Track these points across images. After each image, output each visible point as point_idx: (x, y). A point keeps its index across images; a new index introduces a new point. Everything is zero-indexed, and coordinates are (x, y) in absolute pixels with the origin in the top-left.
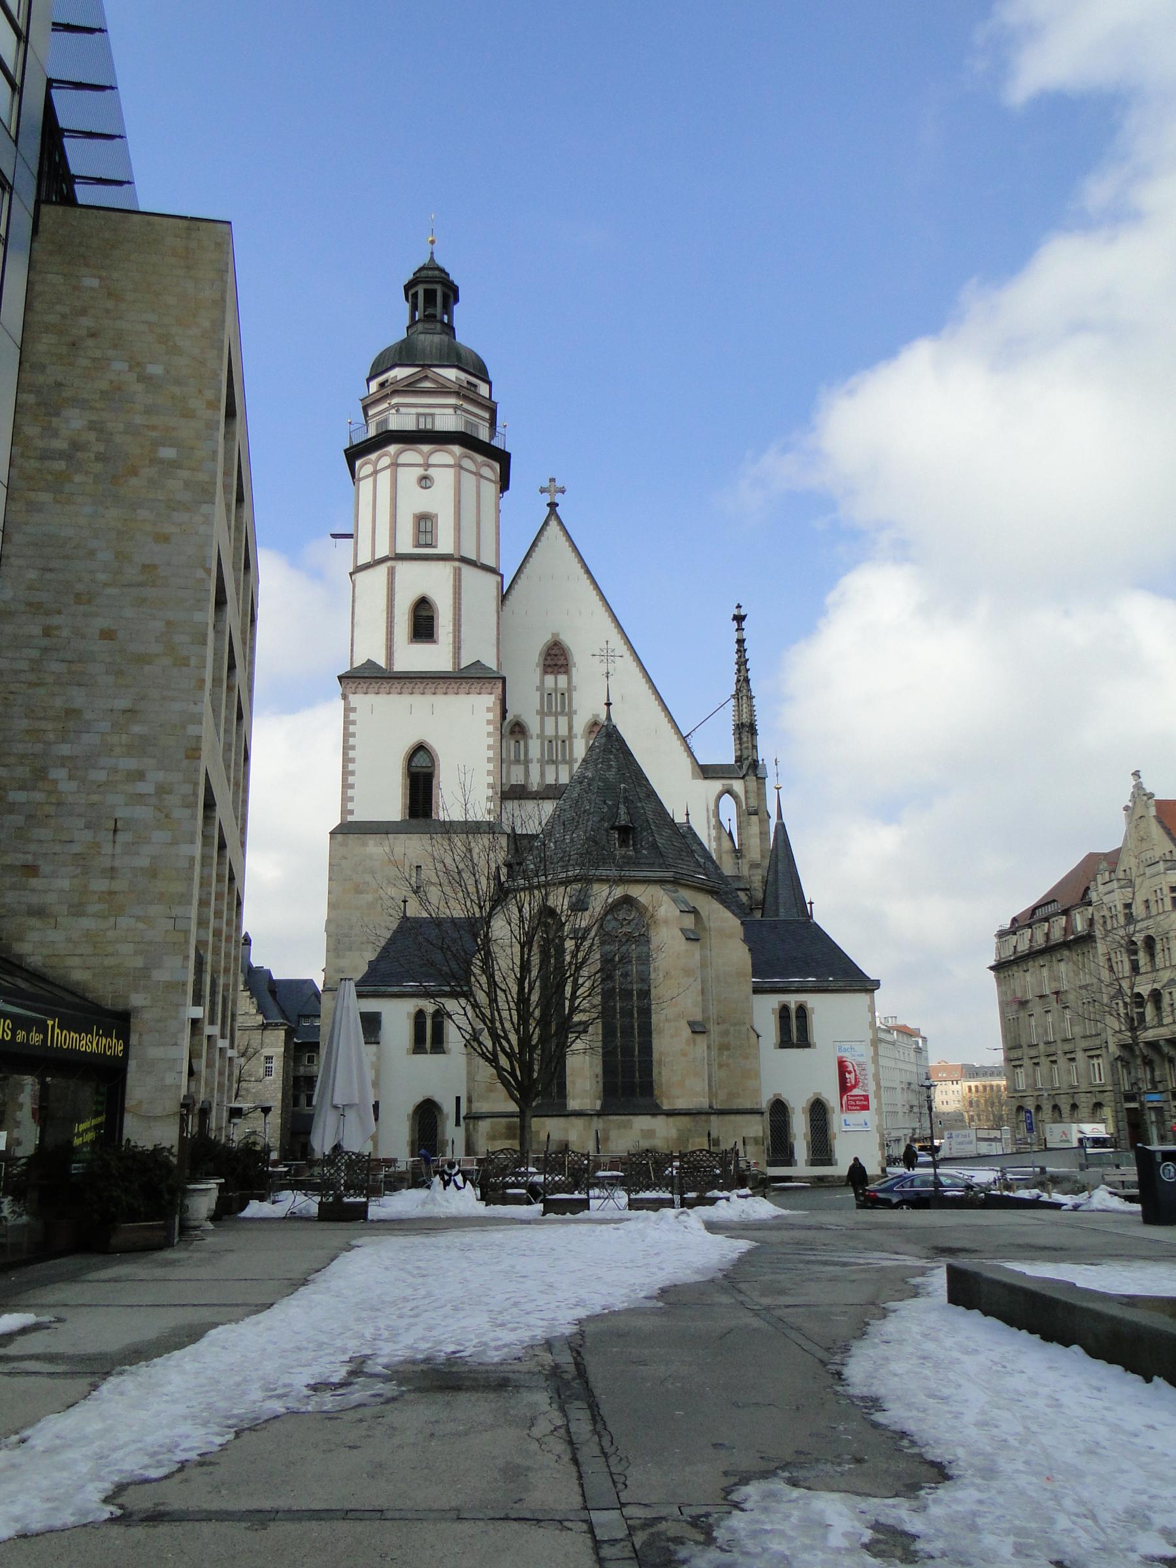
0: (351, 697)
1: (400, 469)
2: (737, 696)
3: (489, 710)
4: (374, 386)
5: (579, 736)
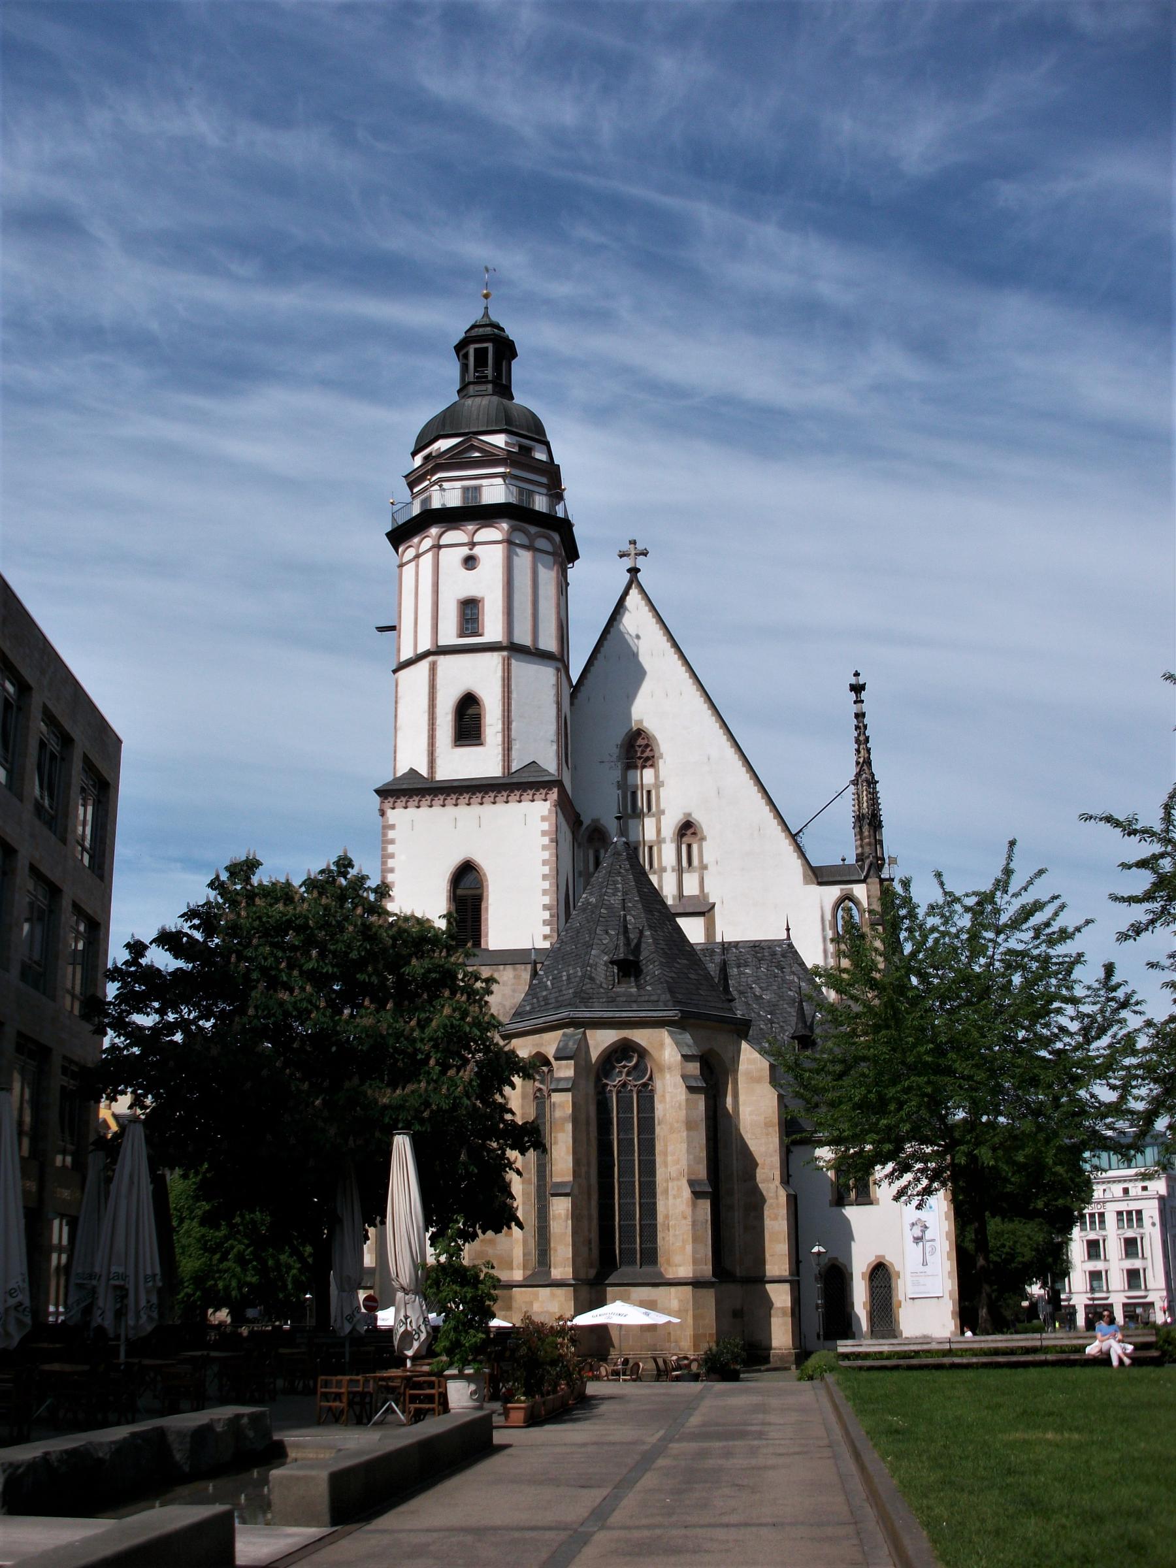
0: (390, 813)
1: (443, 550)
2: (855, 783)
3: (543, 819)
4: (418, 460)
5: (668, 840)
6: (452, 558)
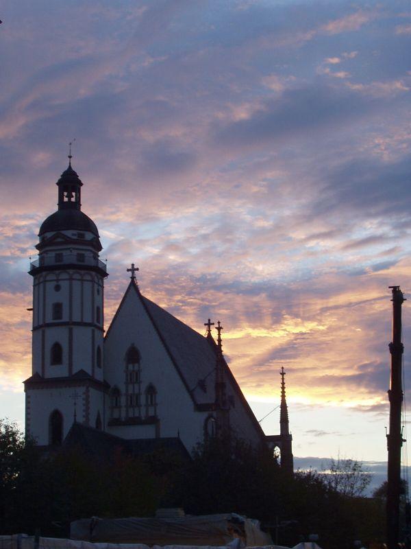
1: (47, 283)
6: (50, 286)
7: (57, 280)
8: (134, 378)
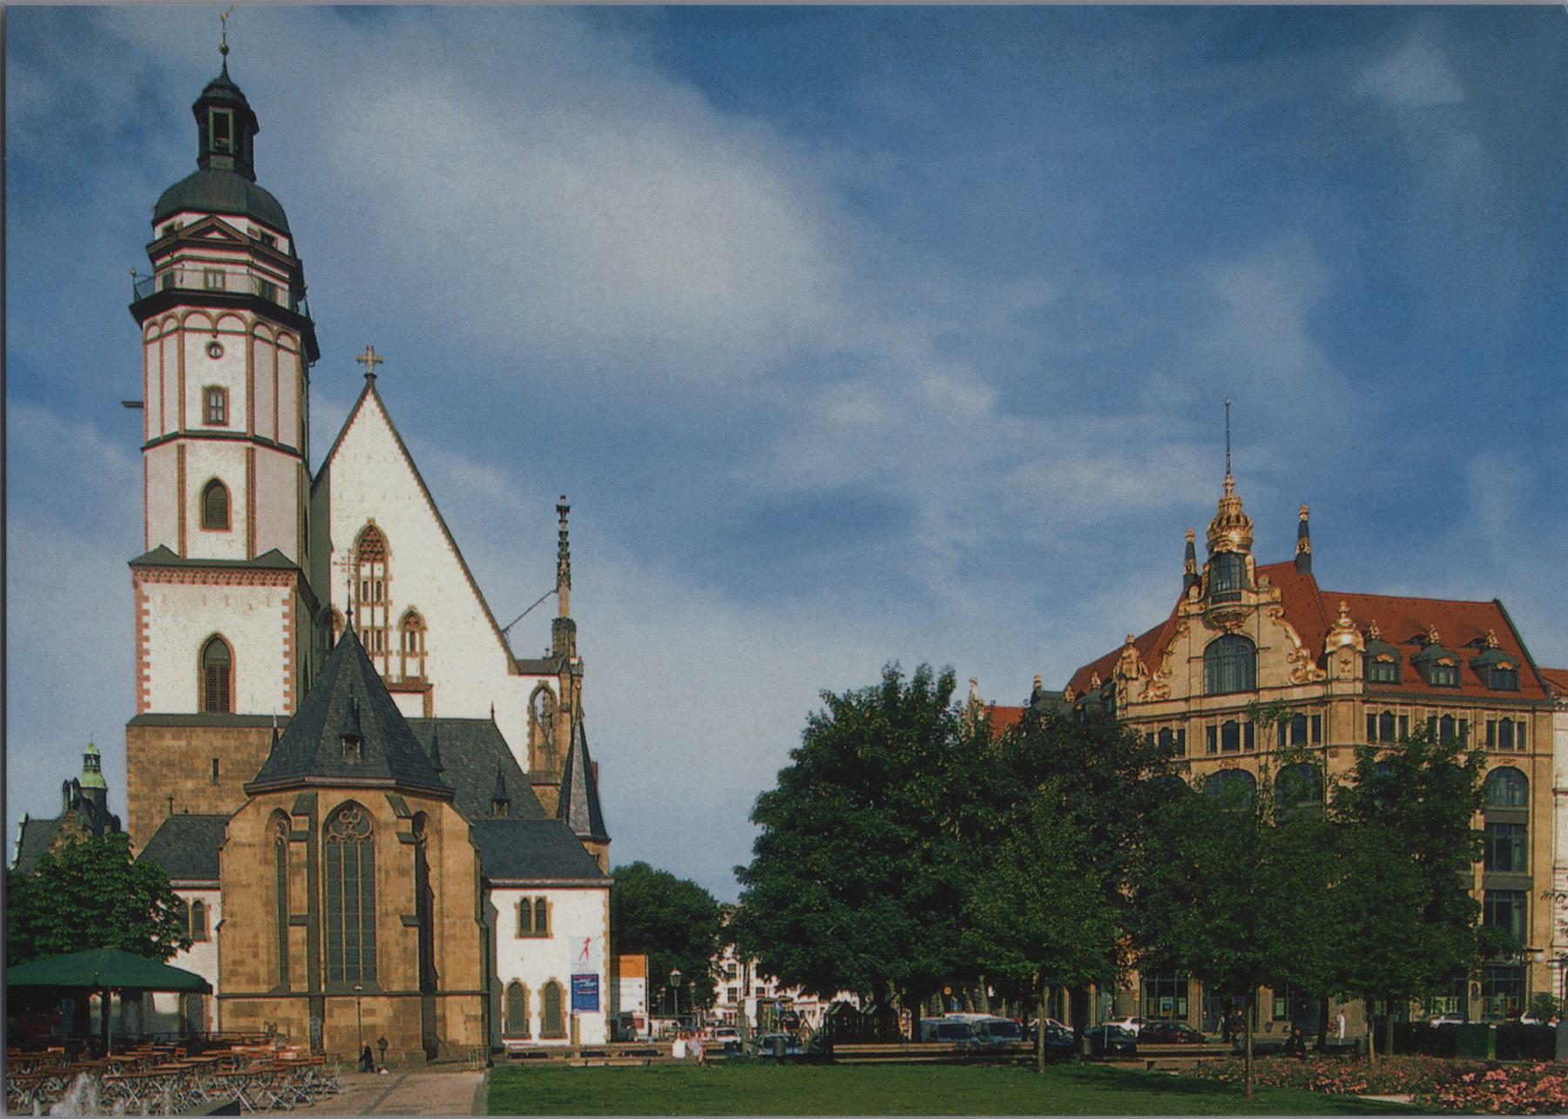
4: (158, 233)
5: (395, 628)
6: (196, 344)
7: (215, 332)
8: (375, 592)
